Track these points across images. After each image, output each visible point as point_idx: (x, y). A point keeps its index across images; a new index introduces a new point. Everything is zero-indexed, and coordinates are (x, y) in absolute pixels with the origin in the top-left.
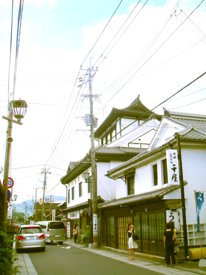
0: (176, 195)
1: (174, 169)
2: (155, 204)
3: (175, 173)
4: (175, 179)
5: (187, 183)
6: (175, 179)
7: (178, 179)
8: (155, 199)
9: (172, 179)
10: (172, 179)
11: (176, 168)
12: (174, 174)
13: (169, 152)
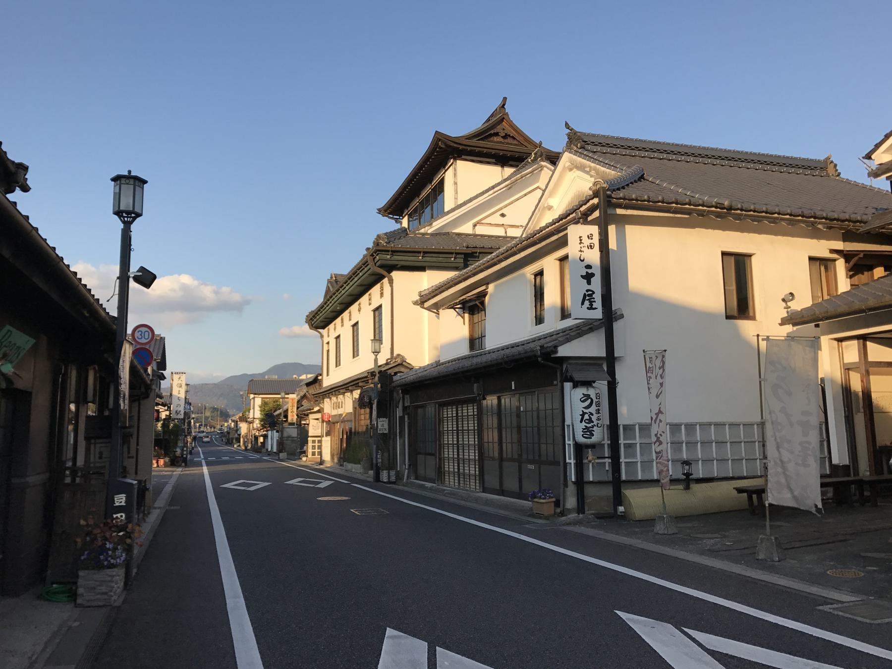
0: (590, 347)
1: (588, 277)
2: (535, 368)
3: (589, 287)
4: (591, 305)
5: (622, 316)
6: (591, 305)
7: (598, 303)
8: (535, 356)
9: (583, 303)
10: (583, 303)
11: (593, 275)
12: (587, 291)
13: (576, 232)
